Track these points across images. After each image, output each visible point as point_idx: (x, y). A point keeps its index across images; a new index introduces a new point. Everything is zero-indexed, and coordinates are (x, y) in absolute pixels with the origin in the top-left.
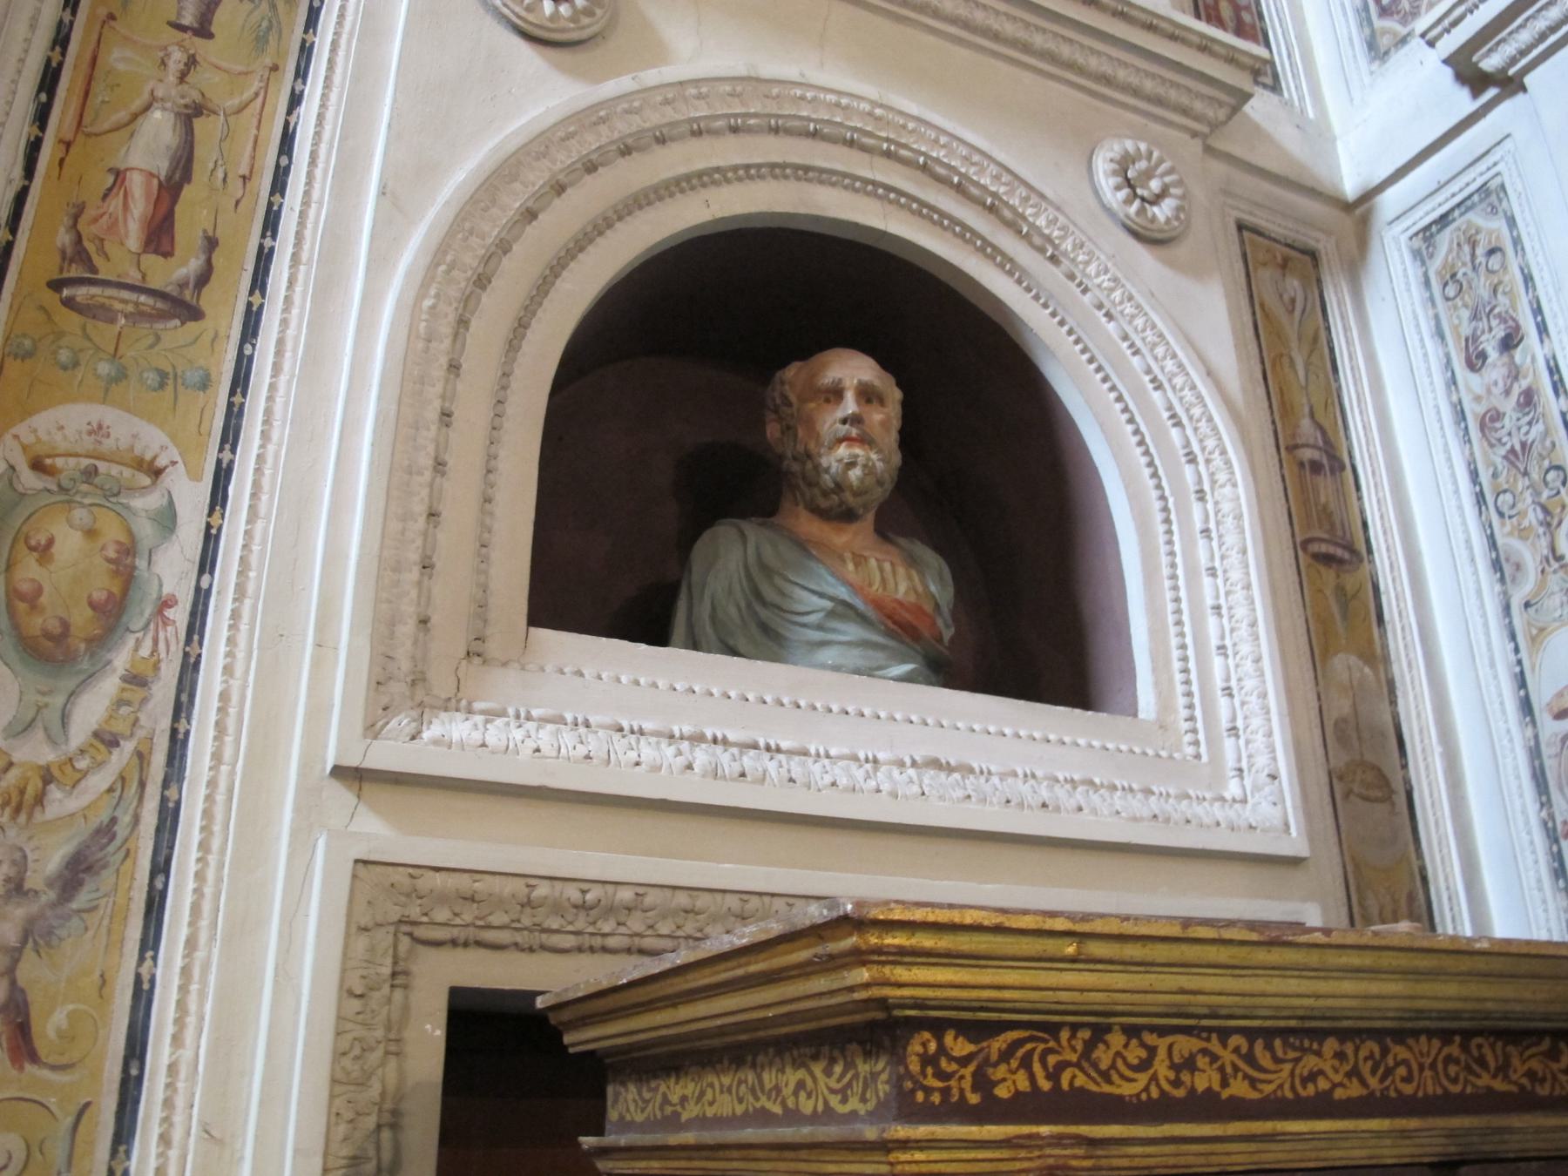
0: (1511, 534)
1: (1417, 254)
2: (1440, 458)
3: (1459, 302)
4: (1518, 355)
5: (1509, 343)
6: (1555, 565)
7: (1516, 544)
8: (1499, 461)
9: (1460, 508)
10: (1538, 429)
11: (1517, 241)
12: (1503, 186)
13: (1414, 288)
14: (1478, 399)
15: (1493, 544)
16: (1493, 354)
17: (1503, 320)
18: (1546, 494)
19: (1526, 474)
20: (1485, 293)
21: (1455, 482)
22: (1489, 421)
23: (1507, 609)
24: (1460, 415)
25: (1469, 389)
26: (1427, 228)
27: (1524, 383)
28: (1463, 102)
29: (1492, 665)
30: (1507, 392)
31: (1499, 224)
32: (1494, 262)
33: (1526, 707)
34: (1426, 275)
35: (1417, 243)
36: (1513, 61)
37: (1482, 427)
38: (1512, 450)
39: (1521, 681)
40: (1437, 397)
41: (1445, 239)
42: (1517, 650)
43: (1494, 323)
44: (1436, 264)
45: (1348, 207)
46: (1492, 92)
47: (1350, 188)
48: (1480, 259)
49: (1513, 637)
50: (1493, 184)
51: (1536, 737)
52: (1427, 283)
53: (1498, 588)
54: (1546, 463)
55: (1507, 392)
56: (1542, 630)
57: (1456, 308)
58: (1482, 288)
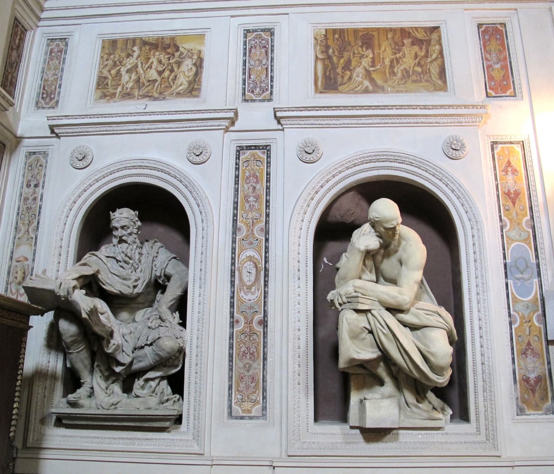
0: (21, 223)
1: (26, 156)
2: (13, 202)
3: (30, 172)
4: (37, 189)
5: (36, 186)
6: (27, 233)
7: (21, 226)
8: (25, 208)
9: (13, 214)
10: (34, 205)
11: (46, 167)
12: (48, 154)
13: (23, 163)
14: (26, 193)
15: (17, 224)
16: (32, 186)
17: (37, 181)
18: (31, 219)
19: (29, 213)
20: (36, 173)
21: (14, 208)
22: (26, 199)
23: (15, 238)
24: (21, 195)
25: (25, 191)
26: (30, 152)
27: (36, 195)
28: (48, 133)
29: (8, 248)
30: (32, 195)
31: (44, 161)
32: (40, 168)
33: (11, 258)
34: (26, 162)
35: (27, 154)
36: (60, 133)
37: (24, 200)
38: (28, 207)
39: (12, 253)
40: (18, 189)
41: (33, 157)
42: (14, 246)
43: (35, 180)
44: (29, 161)
45: (16, 137)
46: (54, 135)
47: (19, 133)
48: (38, 166)
49: (14, 244)
50: (47, 152)
51: (11, 264)
52: (26, 164)
53: (15, 233)
54: (33, 213)
55: (32, 195)
56: (20, 244)
57: (29, 172)
58: (36, 171)
